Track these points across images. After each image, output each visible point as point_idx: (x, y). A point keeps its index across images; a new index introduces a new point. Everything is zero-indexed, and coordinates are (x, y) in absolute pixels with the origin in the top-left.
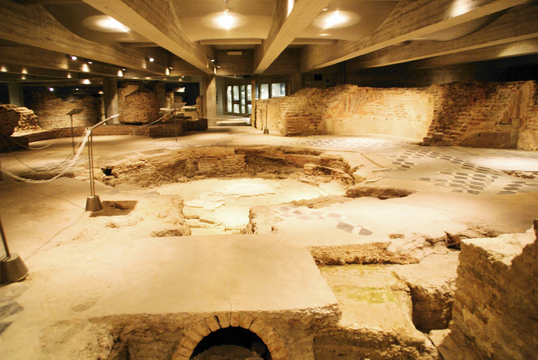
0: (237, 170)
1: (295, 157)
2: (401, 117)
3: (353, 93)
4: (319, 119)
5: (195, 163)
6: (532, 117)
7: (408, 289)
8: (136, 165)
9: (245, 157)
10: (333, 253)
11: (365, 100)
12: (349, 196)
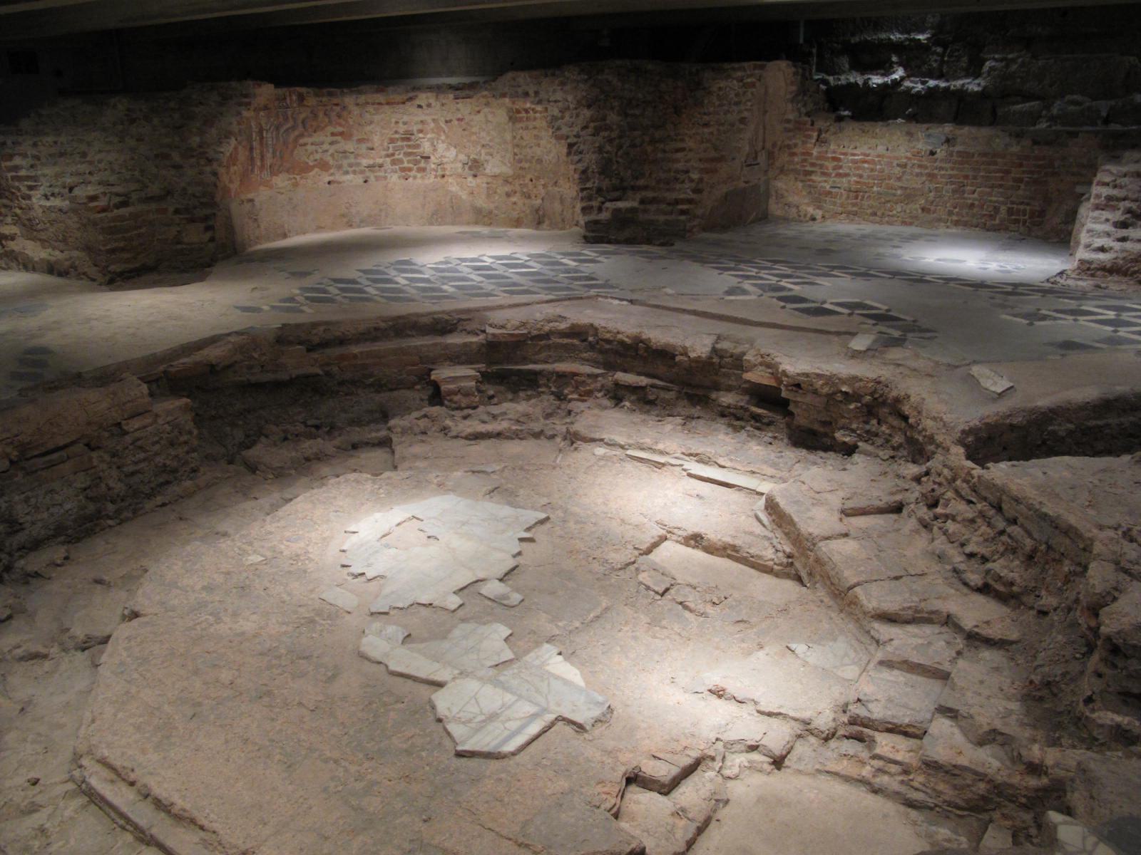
2: (410, 170)
3: (266, 108)
6: (796, 145)
11: (301, 129)
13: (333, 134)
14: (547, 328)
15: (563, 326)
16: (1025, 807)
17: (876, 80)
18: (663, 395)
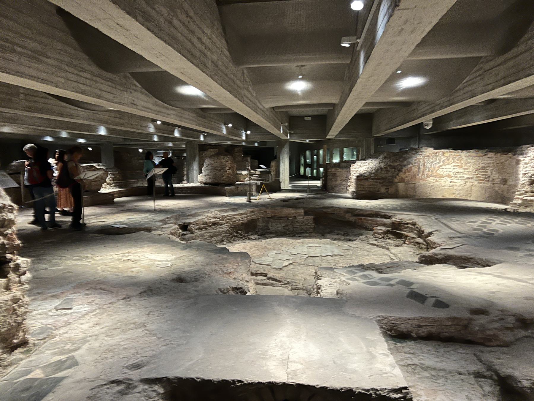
0: (306, 231)
3: (428, 156)
4: (390, 182)
5: (268, 222)
7: (495, 377)
8: (210, 222)
9: (314, 219)
10: (403, 325)
12: (421, 262)
13: (454, 166)
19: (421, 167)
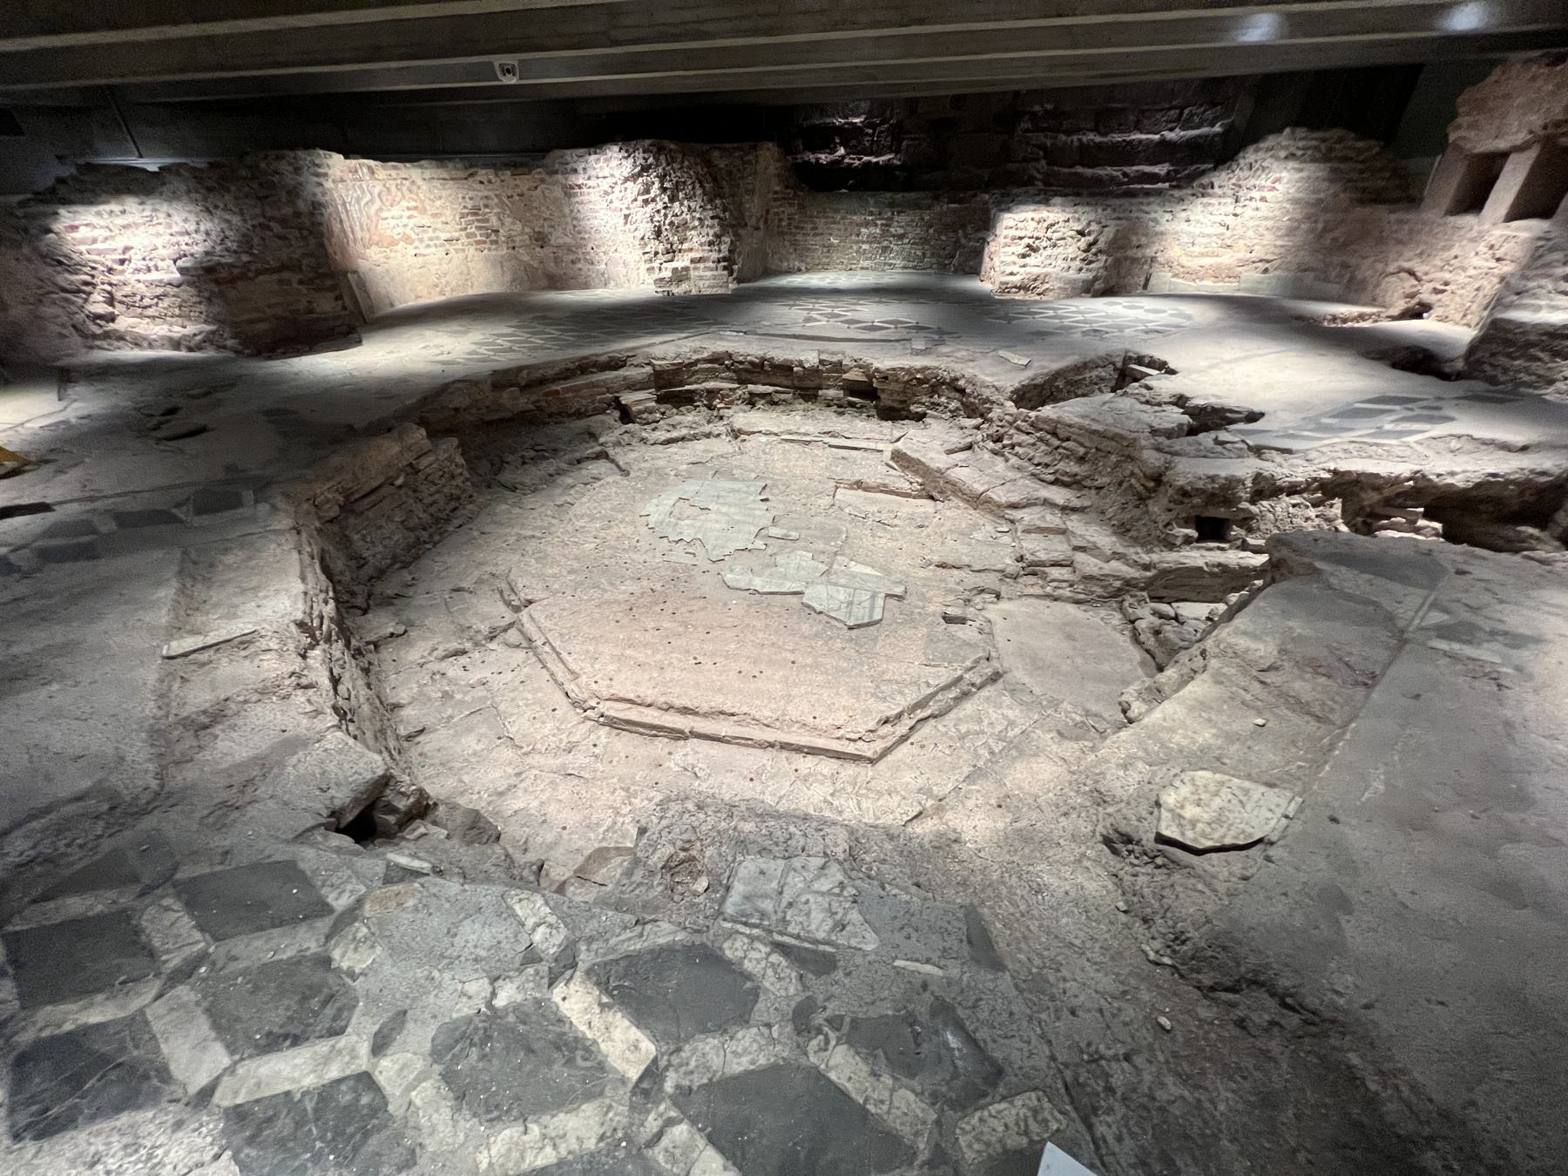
1: (567, 390)
4: (326, 276)
11: (378, 204)
14: (695, 357)
15: (705, 355)
16: (1142, 589)
17: (824, 158)
18: (783, 396)
19: (344, 216)
